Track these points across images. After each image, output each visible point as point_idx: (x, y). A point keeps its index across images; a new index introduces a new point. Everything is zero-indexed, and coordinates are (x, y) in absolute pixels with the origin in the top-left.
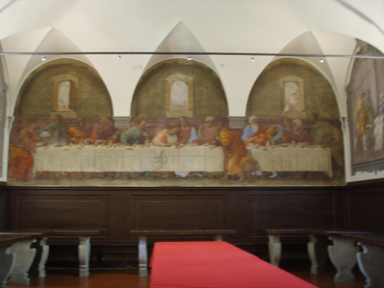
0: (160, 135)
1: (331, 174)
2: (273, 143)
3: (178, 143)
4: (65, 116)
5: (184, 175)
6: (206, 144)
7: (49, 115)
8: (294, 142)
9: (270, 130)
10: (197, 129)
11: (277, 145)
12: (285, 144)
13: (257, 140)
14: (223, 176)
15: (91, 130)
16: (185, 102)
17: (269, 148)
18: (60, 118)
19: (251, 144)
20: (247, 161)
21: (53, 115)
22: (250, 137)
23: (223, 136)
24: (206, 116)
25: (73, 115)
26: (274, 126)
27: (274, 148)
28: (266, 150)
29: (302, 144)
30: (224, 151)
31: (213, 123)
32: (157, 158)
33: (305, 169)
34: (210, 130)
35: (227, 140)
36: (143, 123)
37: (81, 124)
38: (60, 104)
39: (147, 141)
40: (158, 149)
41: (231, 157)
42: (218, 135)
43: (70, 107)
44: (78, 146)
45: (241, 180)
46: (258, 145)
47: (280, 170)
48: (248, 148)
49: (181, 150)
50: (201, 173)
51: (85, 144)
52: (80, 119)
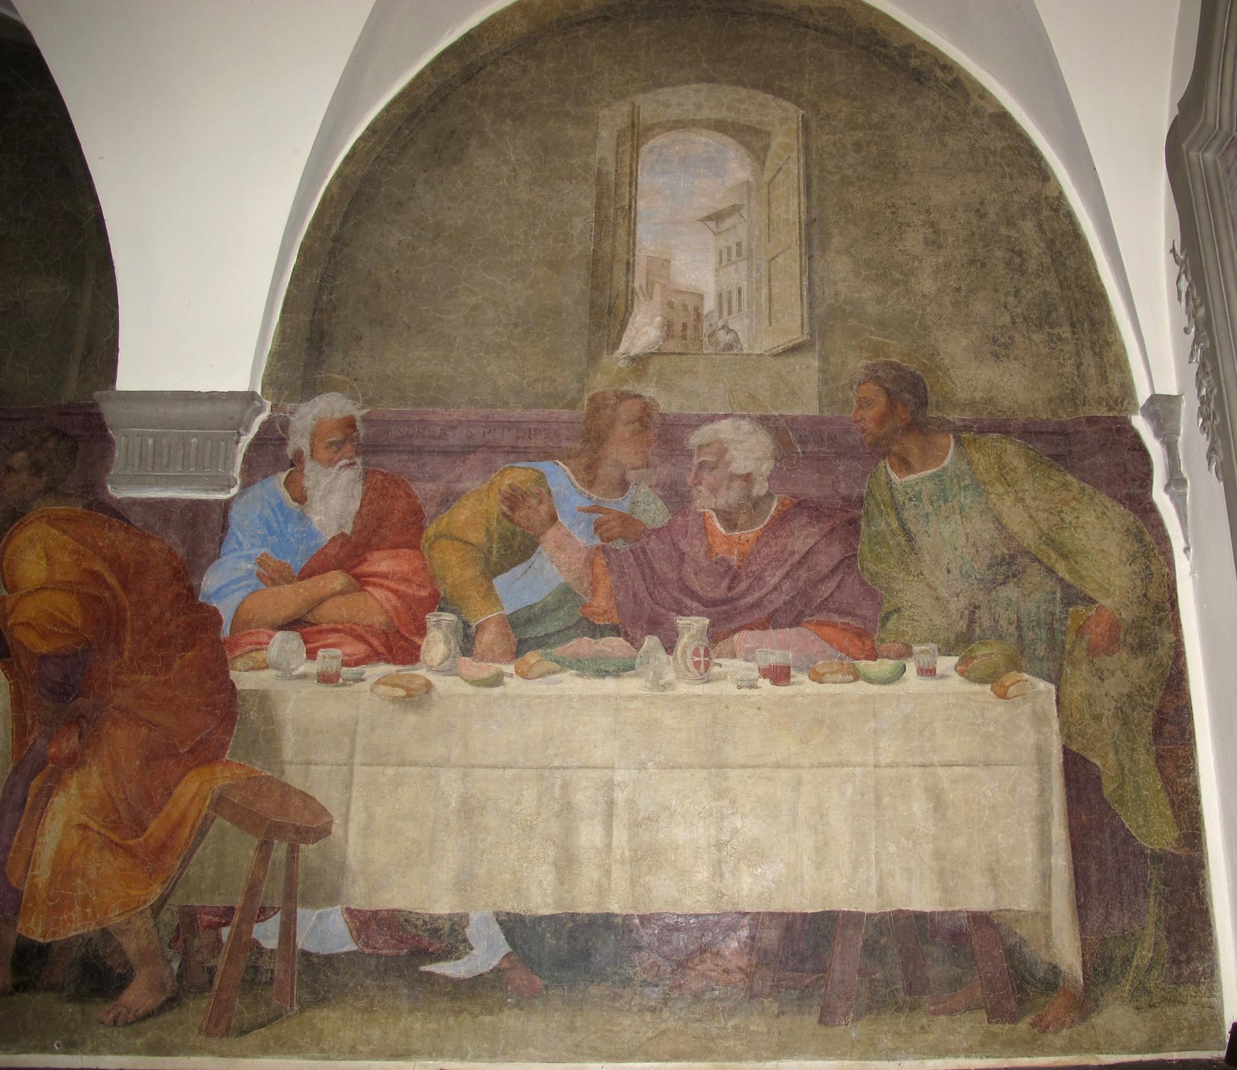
11: (531, 657)
12: (615, 645)
13: (328, 612)
17: (443, 684)
19: (285, 645)
20: (220, 802)
22: (273, 575)
26: (517, 475)
33: (803, 902)
35: (66, 606)
41: (74, 761)
45: (137, 995)
46: (359, 649)
48: (244, 679)
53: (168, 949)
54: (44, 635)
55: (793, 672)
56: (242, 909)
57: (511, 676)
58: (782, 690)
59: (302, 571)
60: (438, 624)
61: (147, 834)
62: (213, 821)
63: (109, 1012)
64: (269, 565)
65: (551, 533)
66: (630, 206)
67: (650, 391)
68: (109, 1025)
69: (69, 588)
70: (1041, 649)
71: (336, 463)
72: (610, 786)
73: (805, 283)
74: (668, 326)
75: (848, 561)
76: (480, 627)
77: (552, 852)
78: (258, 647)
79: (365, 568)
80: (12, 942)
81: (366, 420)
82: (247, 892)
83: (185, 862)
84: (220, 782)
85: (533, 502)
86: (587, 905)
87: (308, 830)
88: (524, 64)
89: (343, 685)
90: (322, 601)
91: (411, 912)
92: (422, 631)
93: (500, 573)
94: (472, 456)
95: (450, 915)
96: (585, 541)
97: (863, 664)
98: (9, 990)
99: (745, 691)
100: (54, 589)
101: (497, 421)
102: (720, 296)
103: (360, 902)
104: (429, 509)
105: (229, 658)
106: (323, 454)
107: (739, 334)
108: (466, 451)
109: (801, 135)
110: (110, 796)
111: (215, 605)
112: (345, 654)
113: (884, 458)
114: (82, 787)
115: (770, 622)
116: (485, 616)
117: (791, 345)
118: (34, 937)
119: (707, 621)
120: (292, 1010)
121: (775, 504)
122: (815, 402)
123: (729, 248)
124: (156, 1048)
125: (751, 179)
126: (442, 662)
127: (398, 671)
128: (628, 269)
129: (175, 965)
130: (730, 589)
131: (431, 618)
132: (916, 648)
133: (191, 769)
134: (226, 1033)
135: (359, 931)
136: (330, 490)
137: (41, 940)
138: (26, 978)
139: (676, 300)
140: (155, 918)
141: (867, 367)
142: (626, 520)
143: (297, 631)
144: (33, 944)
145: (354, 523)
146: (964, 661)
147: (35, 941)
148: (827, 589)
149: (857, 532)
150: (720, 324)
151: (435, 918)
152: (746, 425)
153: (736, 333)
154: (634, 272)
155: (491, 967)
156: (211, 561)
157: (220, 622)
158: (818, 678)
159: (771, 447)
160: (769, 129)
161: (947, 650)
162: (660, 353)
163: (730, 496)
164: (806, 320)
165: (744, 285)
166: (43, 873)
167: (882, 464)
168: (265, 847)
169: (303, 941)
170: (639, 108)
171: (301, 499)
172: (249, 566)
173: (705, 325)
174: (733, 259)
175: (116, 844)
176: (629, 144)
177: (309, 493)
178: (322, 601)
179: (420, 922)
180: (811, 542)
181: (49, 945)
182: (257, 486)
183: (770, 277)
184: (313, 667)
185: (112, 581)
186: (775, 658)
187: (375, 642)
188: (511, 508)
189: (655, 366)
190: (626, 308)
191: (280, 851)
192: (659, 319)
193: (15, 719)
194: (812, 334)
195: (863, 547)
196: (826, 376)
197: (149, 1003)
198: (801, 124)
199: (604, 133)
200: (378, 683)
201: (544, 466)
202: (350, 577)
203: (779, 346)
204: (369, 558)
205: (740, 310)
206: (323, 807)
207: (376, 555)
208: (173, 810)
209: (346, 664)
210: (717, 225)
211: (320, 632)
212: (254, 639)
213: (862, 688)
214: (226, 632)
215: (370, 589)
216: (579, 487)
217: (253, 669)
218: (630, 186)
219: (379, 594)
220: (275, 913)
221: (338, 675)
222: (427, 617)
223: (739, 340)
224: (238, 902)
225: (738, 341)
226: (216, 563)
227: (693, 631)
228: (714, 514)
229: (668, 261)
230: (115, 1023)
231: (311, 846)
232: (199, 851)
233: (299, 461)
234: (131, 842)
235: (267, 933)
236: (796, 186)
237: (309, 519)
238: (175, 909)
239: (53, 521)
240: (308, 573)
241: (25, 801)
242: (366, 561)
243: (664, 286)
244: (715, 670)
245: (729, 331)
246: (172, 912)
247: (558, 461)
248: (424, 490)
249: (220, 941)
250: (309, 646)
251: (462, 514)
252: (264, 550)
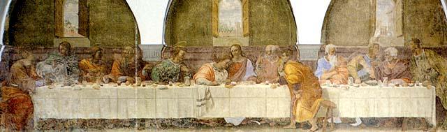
0: (205, 69)
1: (434, 122)
2: (358, 80)
3: (229, 80)
4: (74, 44)
5: (237, 123)
6: (267, 82)
7: (52, 44)
9: (353, 63)
10: (254, 62)
12: (375, 81)
14: (289, 124)
15: (111, 62)
16: (238, 26)
17: (351, 87)
18: (68, 46)
21: (57, 42)
23: (290, 71)
24: (266, 43)
25: (86, 42)
27: (358, 86)
29: (397, 81)
31: (278, 53)
32: (201, 100)
36: (182, 52)
37: (97, 54)
38: (66, 28)
39: (187, 78)
40: (202, 89)
43: (80, 32)
44: (95, 85)
48: (323, 87)
49: (232, 90)
50: (260, 120)
51: (104, 82)
52: (95, 48)
69: (295, 74)
115: (397, 78)
169: (334, 122)
208: (314, 105)
235: (329, 121)
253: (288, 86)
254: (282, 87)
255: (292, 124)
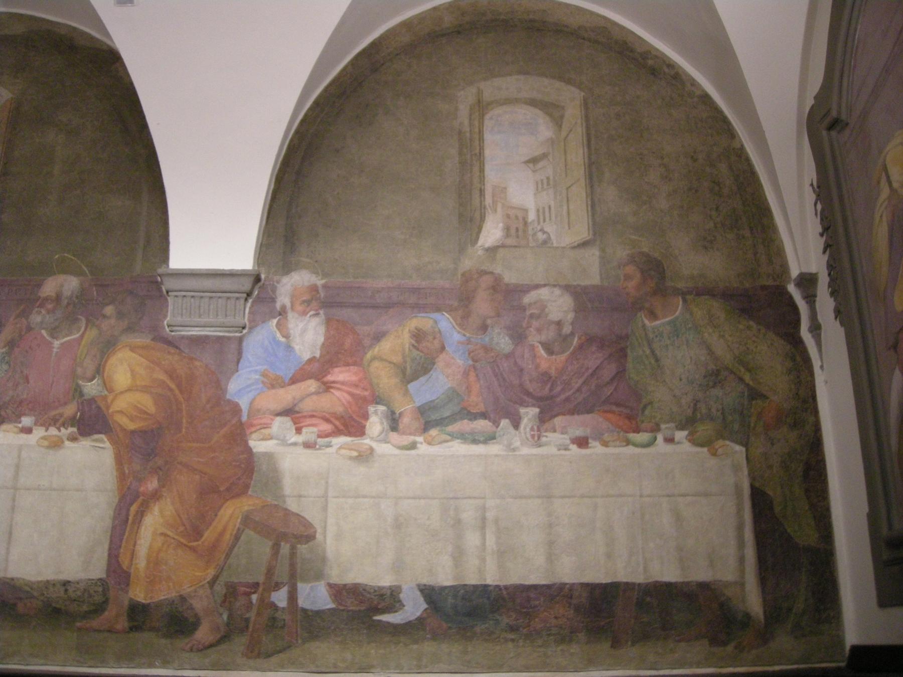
6: (27, 421)
8: (529, 414)
11: (434, 432)
12: (482, 424)
13: (307, 406)
14: (99, 609)
17: (382, 448)
19: (282, 425)
20: (247, 520)
22: (274, 383)
24: (46, 270)
27: (413, 446)
28: (365, 457)
29: (578, 425)
30: (119, 460)
33: (598, 576)
34: (57, 343)
35: (147, 402)
41: (156, 496)
42: (99, 371)
45: (203, 634)
46: (326, 427)
47: (445, 578)
48: (258, 445)
53: (220, 608)
54: (132, 419)
55: (590, 441)
56: (264, 584)
57: (421, 443)
58: (584, 451)
59: (291, 379)
60: (376, 412)
61: (203, 538)
62: (243, 531)
63: (187, 644)
64: (269, 377)
65: (442, 356)
66: (480, 154)
67: (498, 269)
68: (188, 652)
69: (145, 389)
70: (736, 427)
71: (308, 313)
72: (484, 509)
73: (589, 203)
74: (507, 229)
75: (621, 373)
76: (401, 414)
77: (450, 548)
78: (265, 426)
79: (330, 378)
80: (126, 603)
81: (325, 286)
82: (267, 574)
83: (228, 556)
84: (246, 508)
85: (430, 338)
86: (472, 580)
87: (301, 536)
88: (409, 61)
89: (319, 449)
90: (302, 399)
91: (366, 585)
92: (366, 417)
93: (412, 381)
94: (391, 310)
95: (390, 586)
96: (462, 362)
97: (631, 436)
98: (127, 630)
99: (563, 452)
100: (137, 390)
101: (405, 288)
102: (538, 211)
103: (335, 580)
104: (367, 342)
105: (248, 432)
106: (300, 308)
107: (551, 235)
108: (388, 306)
109: (583, 108)
110: (179, 516)
111: (237, 400)
112: (319, 431)
113: (640, 311)
114: (161, 511)
116: (406, 408)
117: (582, 242)
118: (139, 600)
119: (537, 410)
120: (297, 643)
121: (576, 339)
122: (598, 277)
123: (542, 180)
124: (216, 666)
125: (554, 136)
126: (379, 436)
127: (352, 441)
128: (481, 195)
129: (225, 617)
130: (551, 390)
131: (371, 409)
132: (663, 426)
133: (228, 500)
134: (259, 656)
135: (335, 596)
136: (304, 331)
137: (144, 601)
138: (136, 624)
139: (512, 213)
140: (211, 589)
141: (628, 255)
142: (487, 349)
143: (289, 416)
144: (139, 603)
145: (321, 350)
146: (691, 434)
147: (140, 602)
148: (608, 391)
149: (626, 356)
150: (539, 228)
151: (381, 588)
152: (557, 291)
153: (549, 234)
154: (484, 195)
155: (416, 617)
156: (233, 374)
157: (241, 410)
158: (605, 444)
159: (573, 305)
160: (563, 104)
161: (681, 427)
162: (503, 246)
163: (550, 334)
164: (590, 225)
165: (552, 203)
166: (141, 563)
167: (639, 314)
168: (276, 548)
169: (302, 602)
170: (482, 91)
171: (287, 336)
172: (257, 377)
173: (530, 228)
174: (545, 186)
175: (185, 545)
176: (477, 114)
177: (291, 331)
178: (302, 399)
179: (372, 591)
180: (599, 362)
181: (149, 604)
182: (259, 328)
183: (568, 198)
184: (300, 439)
185: (173, 386)
186: (579, 432)
187: (337, 423)
188: (417, 341)
189: (501, 253)
190: (481, 218)
191: (285, 549)
192: (501, 225)
193: (117, 470)
194: (595, 234)
195: (630, 365)
196: (604, 261)
197: (211, 638)
198: (582, 102)
199: (461, 107)
200: (341, 448)
201: (436, 316)
202: (320, 383)
203: (575, 242)
204: (331, 372)
205: (550, 219)
206: (310, 523)
207: (336, 370)
209: (319, 436)
210: (534, 165)
211: (305, 417)
212: (263, 421)
213: (631, 450)
214: (244, 418)
215: (332, 390)
216: (458, 329)
217: (263, 439)
218: (480, 141)
219: (337, 393)
220: (284, 586)
221: (315, 443)
222: (369, 408)
223: (550, 238)
224: (261, 579)
225: (549, 238)
226: (237, 374)
227: (530, 416)
228: (540, 346)
229: (505, 188)
230: (191, 650)
231: (304, 546)
232: (236, 549)
233: (284, 312)
234: (195, 544)
235: (280, 598)
236: (581, 141)
237: (293, 348)
238: (222, 583)
239: (133, 349)
240: (294, 381)
241: (128, 519)
242: (329, 373)
243: (503, 204)
244: (544, 439)
245: (544, 232)
246: (221, 586)
247: (444, 313)
248: (363, 330)
249: (251, 603)
250: (297, 425)
251: (385, 346)
252: (265, 367)
253: (113, 442)
254: (86, 443)
255: (110, 613)
